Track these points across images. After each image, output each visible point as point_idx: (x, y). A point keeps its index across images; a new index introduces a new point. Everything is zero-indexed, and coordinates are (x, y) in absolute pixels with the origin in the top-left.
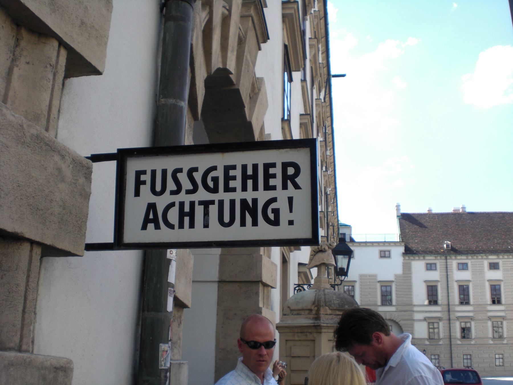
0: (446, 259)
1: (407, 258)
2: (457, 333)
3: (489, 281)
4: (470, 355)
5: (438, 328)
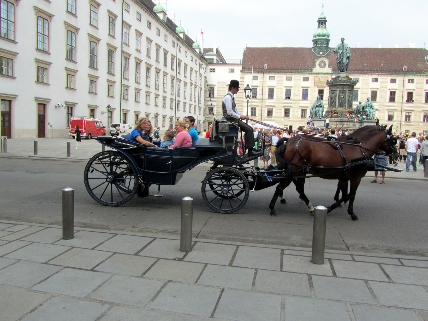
0: (263, 74)
1: (243, 73)
3: (285, 87)
4: (284, 126)
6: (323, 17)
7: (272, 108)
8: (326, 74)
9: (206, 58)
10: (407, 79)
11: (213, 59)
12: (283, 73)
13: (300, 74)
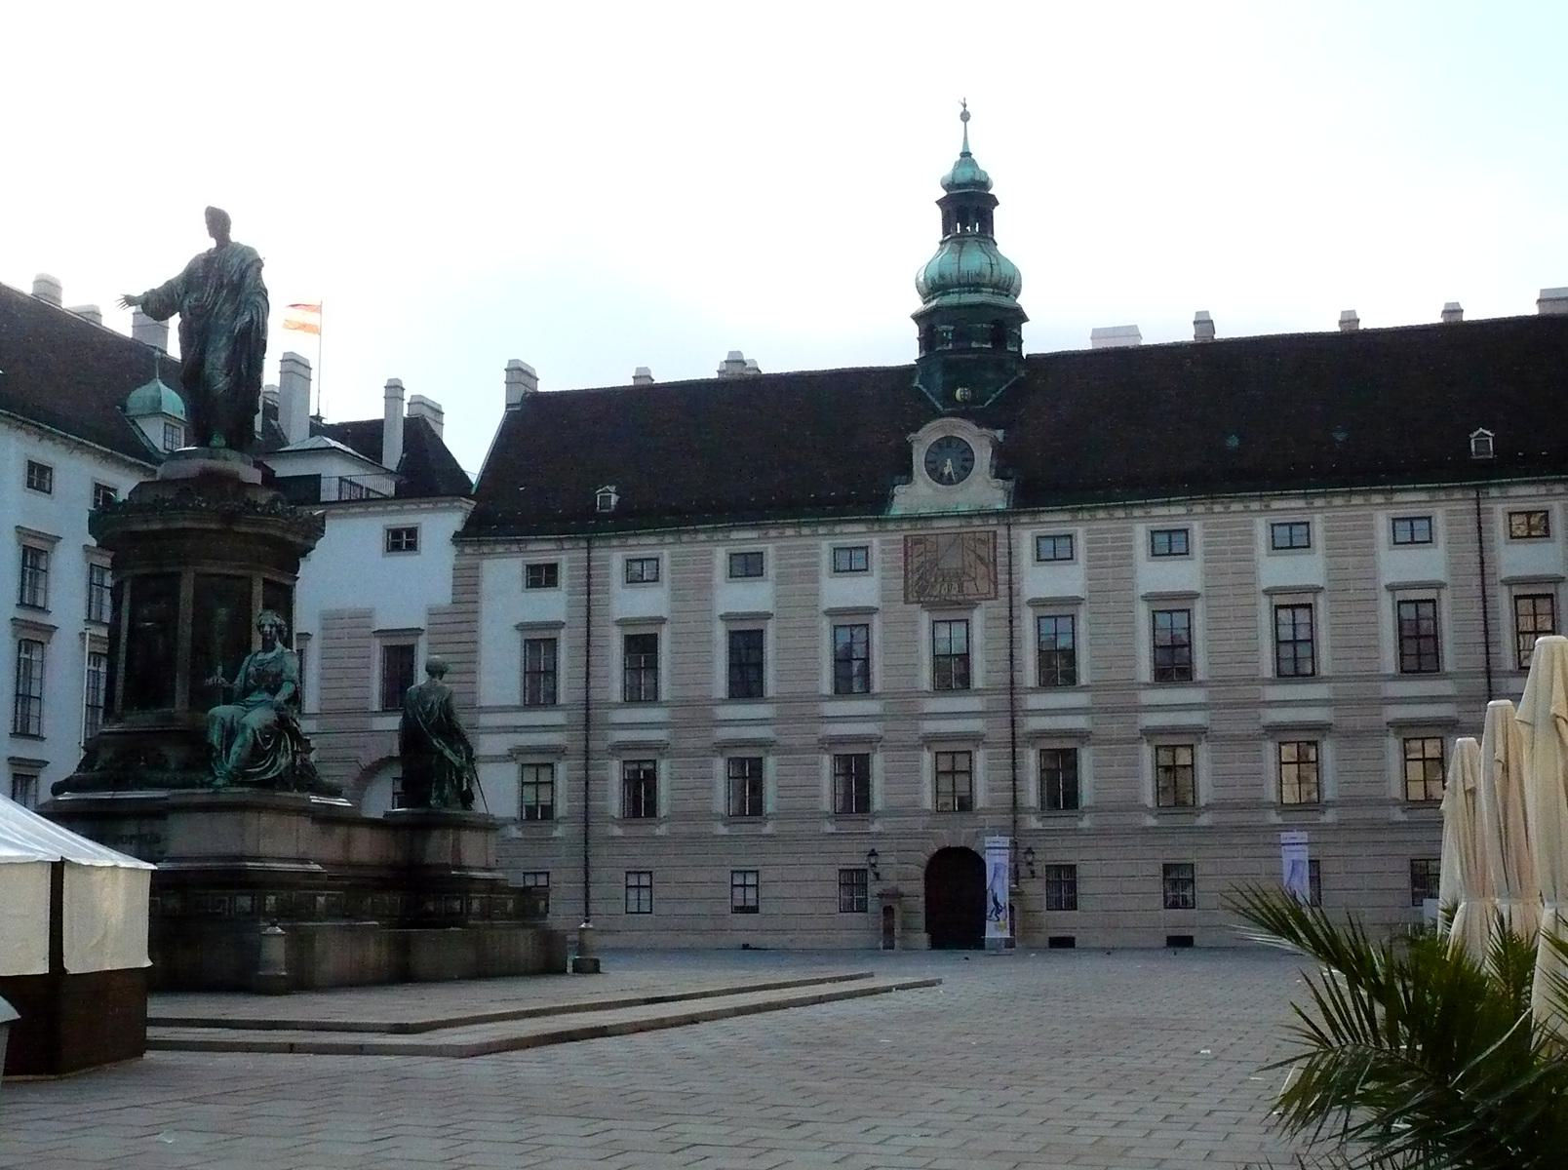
0: (589, 549)
1: (468, 550)
2: (612, 798)
3: (727, 618)
5: (969, 773)
6: (966, 174)
7: (654, 762)
8: (976, 522)
9: (278, 475)
10: (1498, 511)
11: (316, 479)
12: (705, 531)
13: (814, 535)
